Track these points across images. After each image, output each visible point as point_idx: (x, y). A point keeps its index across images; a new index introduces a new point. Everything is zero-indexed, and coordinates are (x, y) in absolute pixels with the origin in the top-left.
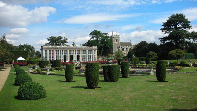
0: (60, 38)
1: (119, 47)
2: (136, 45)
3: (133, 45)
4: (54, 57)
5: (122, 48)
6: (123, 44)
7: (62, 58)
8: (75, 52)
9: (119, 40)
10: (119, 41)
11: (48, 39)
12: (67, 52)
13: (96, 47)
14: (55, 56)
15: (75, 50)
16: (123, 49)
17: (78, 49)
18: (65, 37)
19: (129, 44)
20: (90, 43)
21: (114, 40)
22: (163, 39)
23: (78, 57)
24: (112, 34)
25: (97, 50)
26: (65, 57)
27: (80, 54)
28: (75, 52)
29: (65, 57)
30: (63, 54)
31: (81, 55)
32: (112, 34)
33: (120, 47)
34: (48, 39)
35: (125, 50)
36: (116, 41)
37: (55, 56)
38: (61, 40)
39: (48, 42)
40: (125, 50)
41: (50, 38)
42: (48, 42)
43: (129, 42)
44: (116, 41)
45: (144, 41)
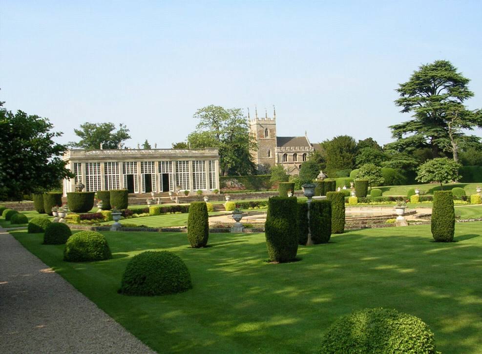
0: (109, 127)
2: (325, 145)
3: (312, 145)
4: (118, 182)
5: (283, 154)
6: (282, 141)
7: (122, 186)
9: (273, 131)
10: (273, 135)
11: (76, 131)
13: (216, 152)
15: (287, 162)
16: (287, 155)
17: (165, 159)
18: (121, 125)
19: (302, 141)
20: (198, 142)
21: (260, 131)
22: (399, 129)
23: (165, 178)
24: (256, 114)
26: (130, 179)
29: (130, 179)
32: (256, 114)
34: (76, 131)
35: (290, 157)
36: (266, 132)
37: (102, 179)
38: (112, 132)
39: (79, 139)
40: (290, 157)
41: (82, 130)
42: (79, 139)
43: (304, 135)
45: (344, 135)
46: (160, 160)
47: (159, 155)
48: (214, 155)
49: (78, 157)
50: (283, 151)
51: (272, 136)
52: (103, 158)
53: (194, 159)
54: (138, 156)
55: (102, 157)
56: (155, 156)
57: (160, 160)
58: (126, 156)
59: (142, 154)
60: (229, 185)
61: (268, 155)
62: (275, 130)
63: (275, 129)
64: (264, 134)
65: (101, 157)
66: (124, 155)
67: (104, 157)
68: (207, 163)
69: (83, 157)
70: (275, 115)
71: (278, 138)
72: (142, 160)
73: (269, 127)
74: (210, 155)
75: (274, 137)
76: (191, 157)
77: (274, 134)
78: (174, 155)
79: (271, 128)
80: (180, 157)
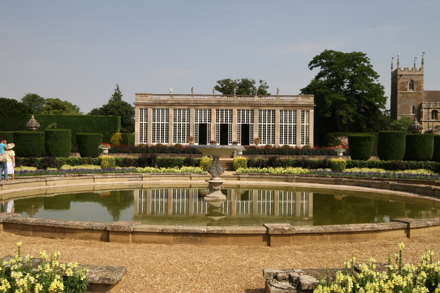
1: (420, 106)
5: (431, 110)
8: (235, 116)
10: (420, 88)
12: (210, 115)
14: (171, 128)
21: (402, 83)
24: (398, 64)
25: (312, 111)
27: (231, 121)
28: (235, 116)
30: (196, 120)
31: (256, 124)
32: (398, 64)
33: (424, 106)
37: (171, 128)
44: (412, 87)
46: (239, 108)
47: (238, 103)
48: (308, 104)
49: (143, 102)
50: (430, 107)
51: (417, 88)
52: (172, 105)
53: (282, 108)
54: (212, 102)
55: (171, 102)
56: (232, 103)
57: (239, 108)
58: (198, 102)
59: (218, 101)
60: (345, 143)
61: (411, 111)
62: (422, 82)
63: (422, 81)
64: (408, 86)
65: (169, 102)
66: (197, 101)
67: (173, 102)
68: (299, 112)
69: (149, 102)
70: (422, 63)
71: (425, 91)
72: (217, 108)
73: (415, 79)
74: (303, 103)
75: (420, 90)
76: (277, 106)
77: (421, 87)
78: (257, 103)
79: (417, 80)
80: (264, 106)
